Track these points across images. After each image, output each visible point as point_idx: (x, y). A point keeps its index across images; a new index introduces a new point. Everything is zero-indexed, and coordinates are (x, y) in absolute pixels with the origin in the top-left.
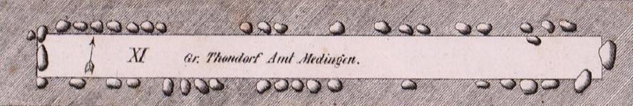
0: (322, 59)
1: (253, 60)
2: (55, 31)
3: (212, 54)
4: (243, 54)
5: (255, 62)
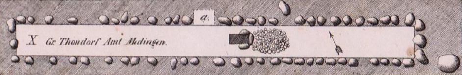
0: (85, 41)
1: (94, 43)
2: (45, 23)
3: (64, 39)
4: (86, 39)
5: (96, 44)
